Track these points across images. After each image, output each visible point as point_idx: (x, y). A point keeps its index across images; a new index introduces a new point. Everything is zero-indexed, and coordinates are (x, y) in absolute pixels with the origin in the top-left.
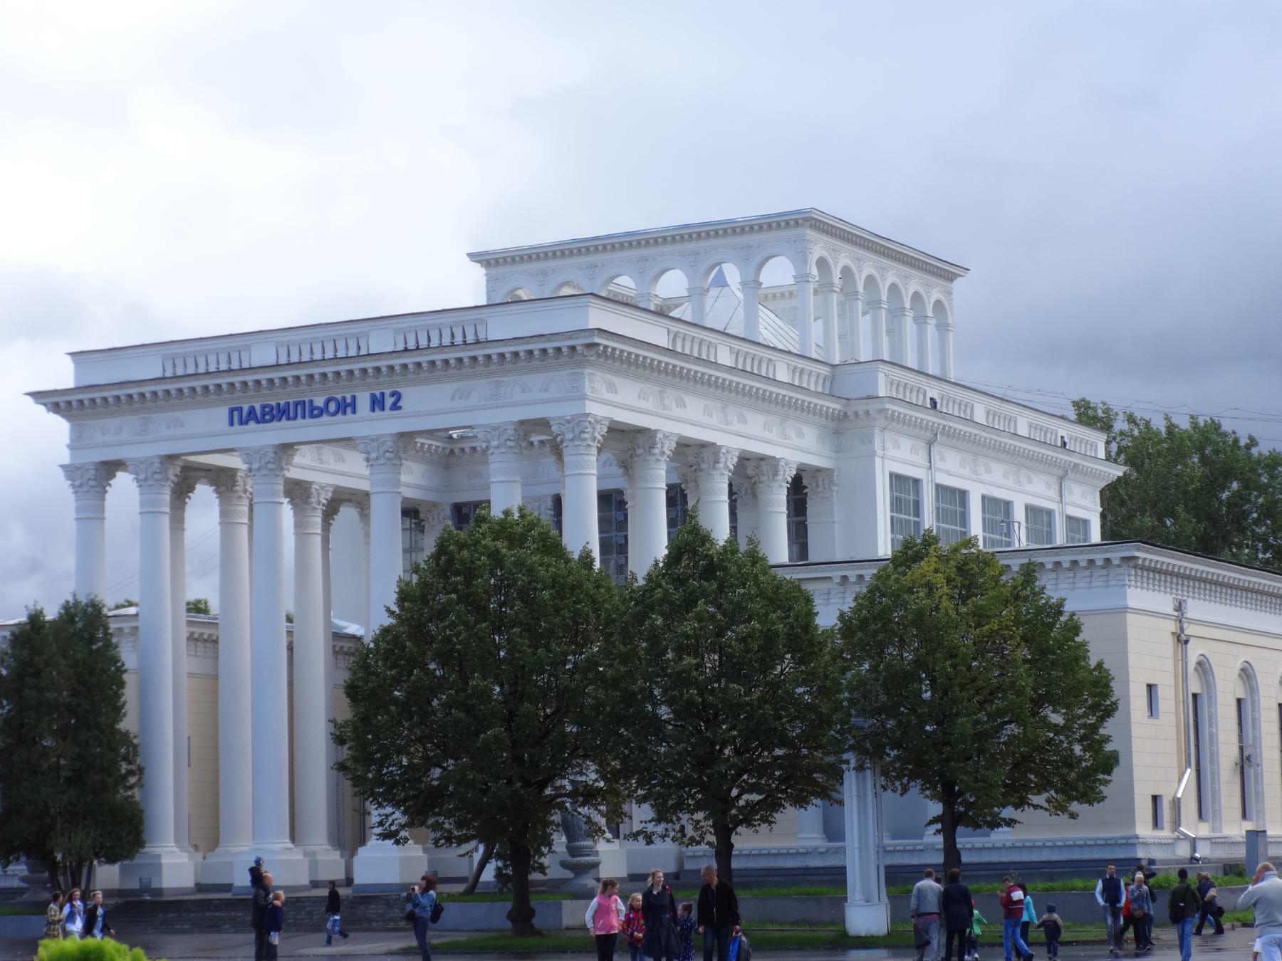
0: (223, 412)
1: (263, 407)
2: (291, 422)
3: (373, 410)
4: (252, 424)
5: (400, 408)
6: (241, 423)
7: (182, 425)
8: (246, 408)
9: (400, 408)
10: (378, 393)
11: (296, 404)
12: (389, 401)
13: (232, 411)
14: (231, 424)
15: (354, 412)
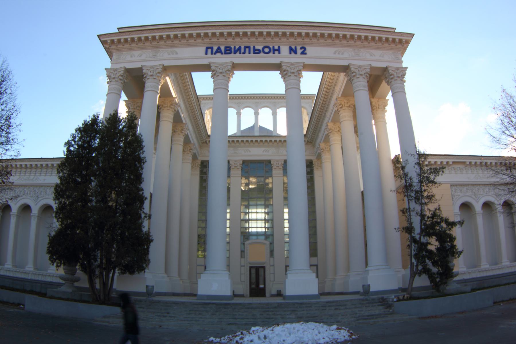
0: (204, 49)
1: (226, 48)
2: (242, 55)
3: (290, 53)
4: (219, 55)
5: (306, 54)
6: (212, 54)
7: (177, 53)
8: (215, 48)
9: (306, 54)
10: (293, 47)
11: (246, 47)
12: (299, 51)
13: (207, 48)
14: (206, 54)
15: (279, 53)
